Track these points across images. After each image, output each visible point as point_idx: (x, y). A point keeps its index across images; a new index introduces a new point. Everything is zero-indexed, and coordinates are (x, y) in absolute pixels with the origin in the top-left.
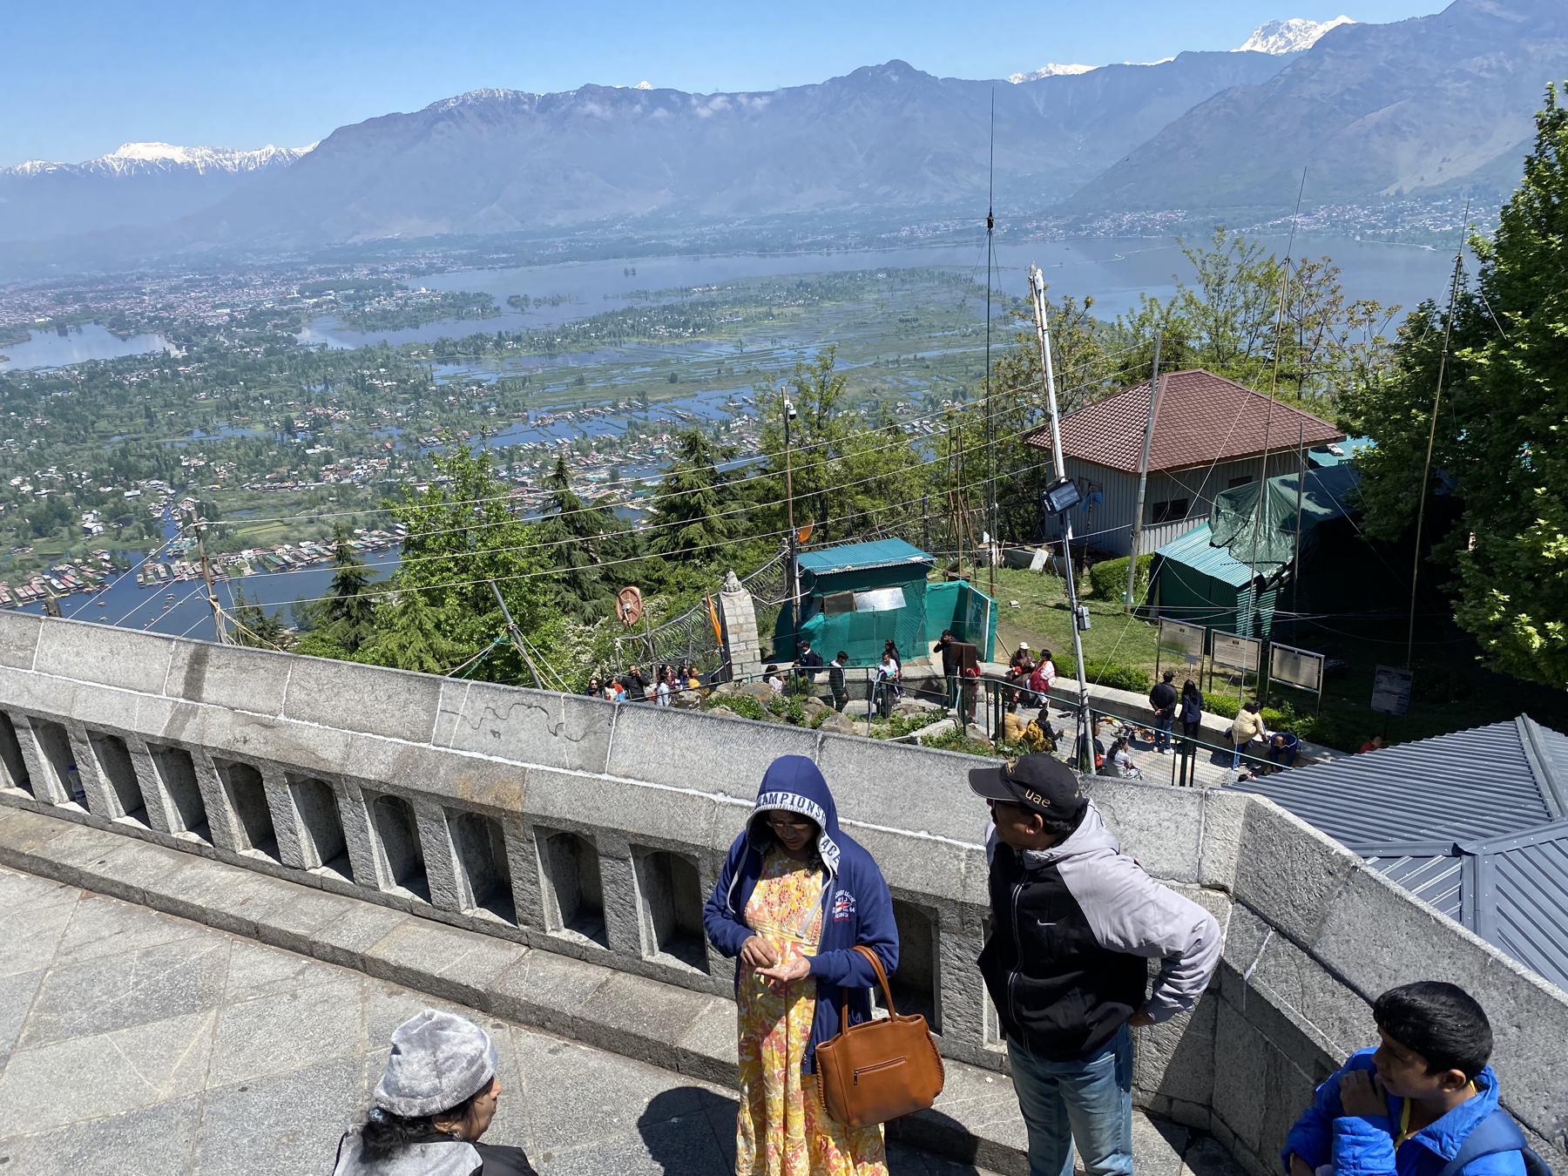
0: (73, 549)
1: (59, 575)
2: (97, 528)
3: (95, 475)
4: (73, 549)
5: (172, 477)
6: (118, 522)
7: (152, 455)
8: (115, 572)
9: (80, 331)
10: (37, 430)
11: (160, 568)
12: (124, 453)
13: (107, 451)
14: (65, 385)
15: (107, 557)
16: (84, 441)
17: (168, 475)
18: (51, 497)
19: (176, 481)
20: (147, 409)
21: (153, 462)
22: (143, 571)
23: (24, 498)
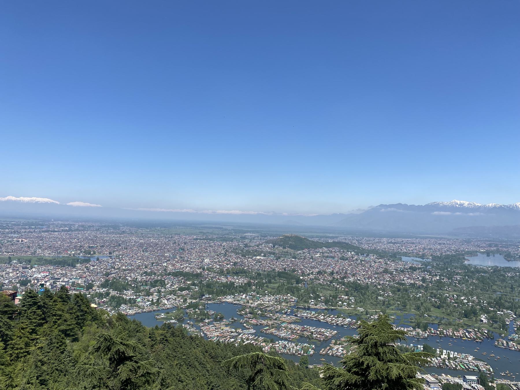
0: (475, 325)
1: (469, 332)
2: (485, 321)
3: (489, 303)
4: (475, 325)
5: (516, 311)
6: (493, 321)
7: (510, 302)
8: (488, 338)
9: (494, 256)
10: (473, 284)
11: (505, 342)
12: (500, 298)
13: (494, 296)
14: (485, 272)
15: (486, 332)
16: (487, 291)
17: (514, 311)
18: (472, 306)
19: (517, 313)
20: (512, 286)
21: (510, 304)
22: (498, 341)
23: (464, 304)
